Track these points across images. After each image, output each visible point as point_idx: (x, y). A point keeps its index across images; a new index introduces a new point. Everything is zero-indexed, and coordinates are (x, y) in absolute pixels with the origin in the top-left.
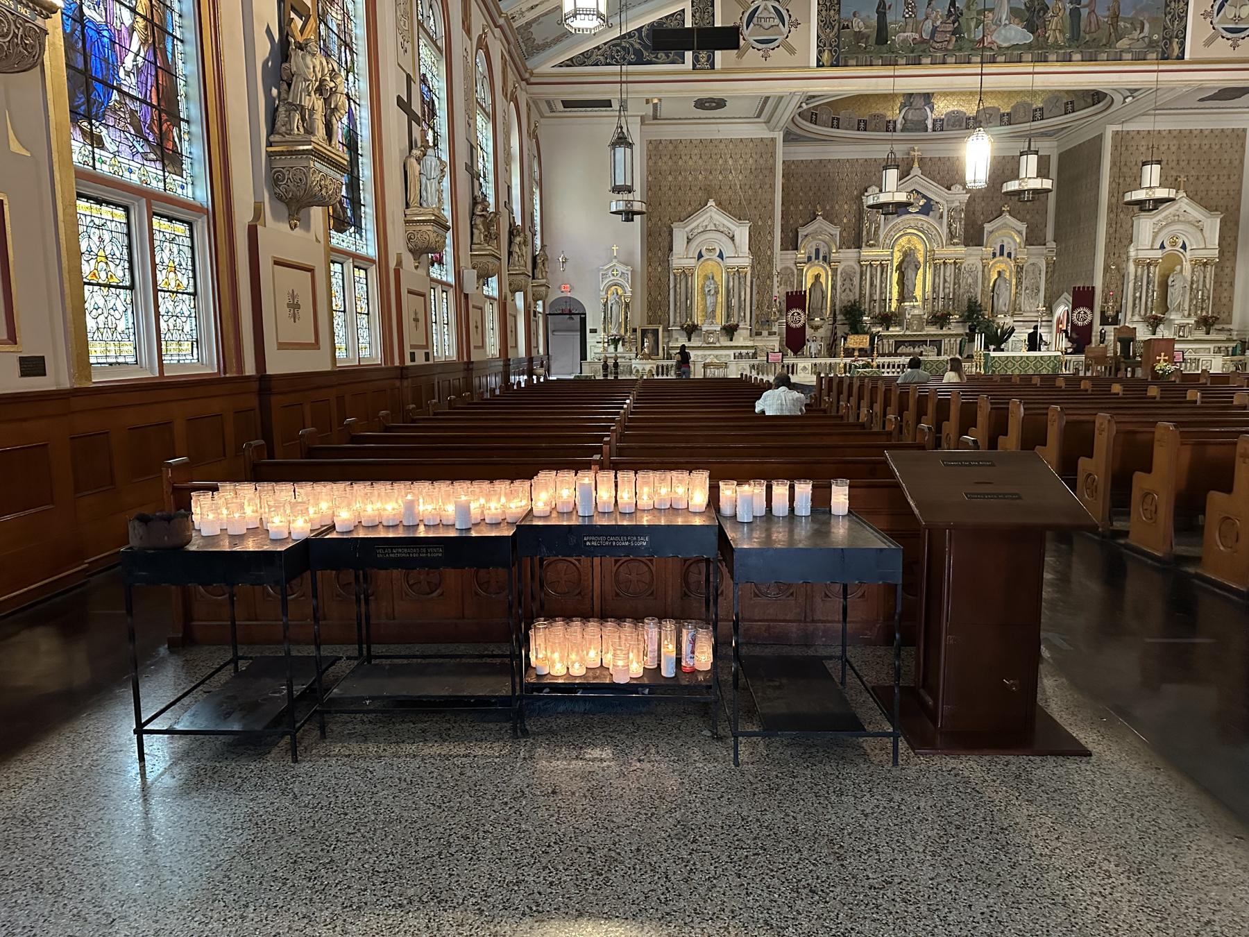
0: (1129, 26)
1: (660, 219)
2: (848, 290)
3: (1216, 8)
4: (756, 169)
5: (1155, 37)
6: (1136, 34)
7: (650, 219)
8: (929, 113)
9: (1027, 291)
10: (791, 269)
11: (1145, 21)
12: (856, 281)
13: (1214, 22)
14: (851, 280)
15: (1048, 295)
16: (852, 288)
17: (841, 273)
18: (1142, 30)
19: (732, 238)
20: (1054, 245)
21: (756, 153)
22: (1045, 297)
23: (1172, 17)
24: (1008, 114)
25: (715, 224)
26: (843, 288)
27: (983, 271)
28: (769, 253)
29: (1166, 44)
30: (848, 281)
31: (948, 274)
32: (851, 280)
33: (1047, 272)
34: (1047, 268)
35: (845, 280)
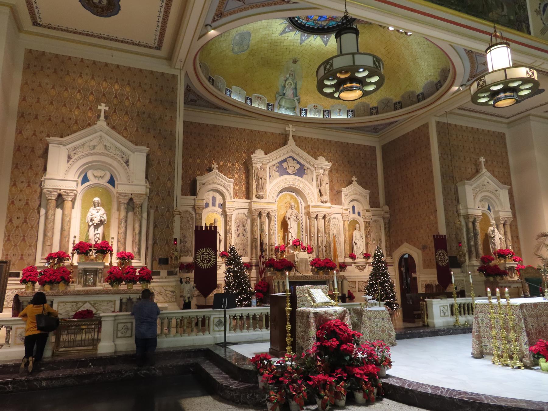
0: (494, 3)
1: (34, 134)
2: (241, 235)
3: (542, 9)
4: (156, 100)
5: (512, 18)
6: (499, 11)
7: (20, 132)
8: (297, 105)
9: (374, 242)
10: (190, 213)
11: (504, 4)
12: (248, 228)
13: (543, 19)
14: (244, 226)
15: (388, 246)
16: (245, 233)
17: (236, 220)
18: (503, 10)
19: (127, 162)
20: (386, 208)
21: (157, 86)
22: (386, 247)
23: (519, 6)
24: (352, 111)
25: (105, 146)
26: (238, 233)
27: (344, 225)
28: (169, 185)
29: (519, 24)
30: (241, 228)
31: (320, 225)
32: (244, 226)
33: (385, 228)
34: (385, 225)
35: (239, 226)
